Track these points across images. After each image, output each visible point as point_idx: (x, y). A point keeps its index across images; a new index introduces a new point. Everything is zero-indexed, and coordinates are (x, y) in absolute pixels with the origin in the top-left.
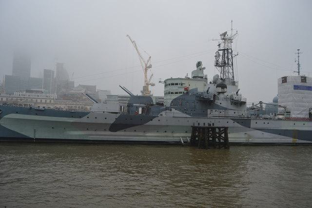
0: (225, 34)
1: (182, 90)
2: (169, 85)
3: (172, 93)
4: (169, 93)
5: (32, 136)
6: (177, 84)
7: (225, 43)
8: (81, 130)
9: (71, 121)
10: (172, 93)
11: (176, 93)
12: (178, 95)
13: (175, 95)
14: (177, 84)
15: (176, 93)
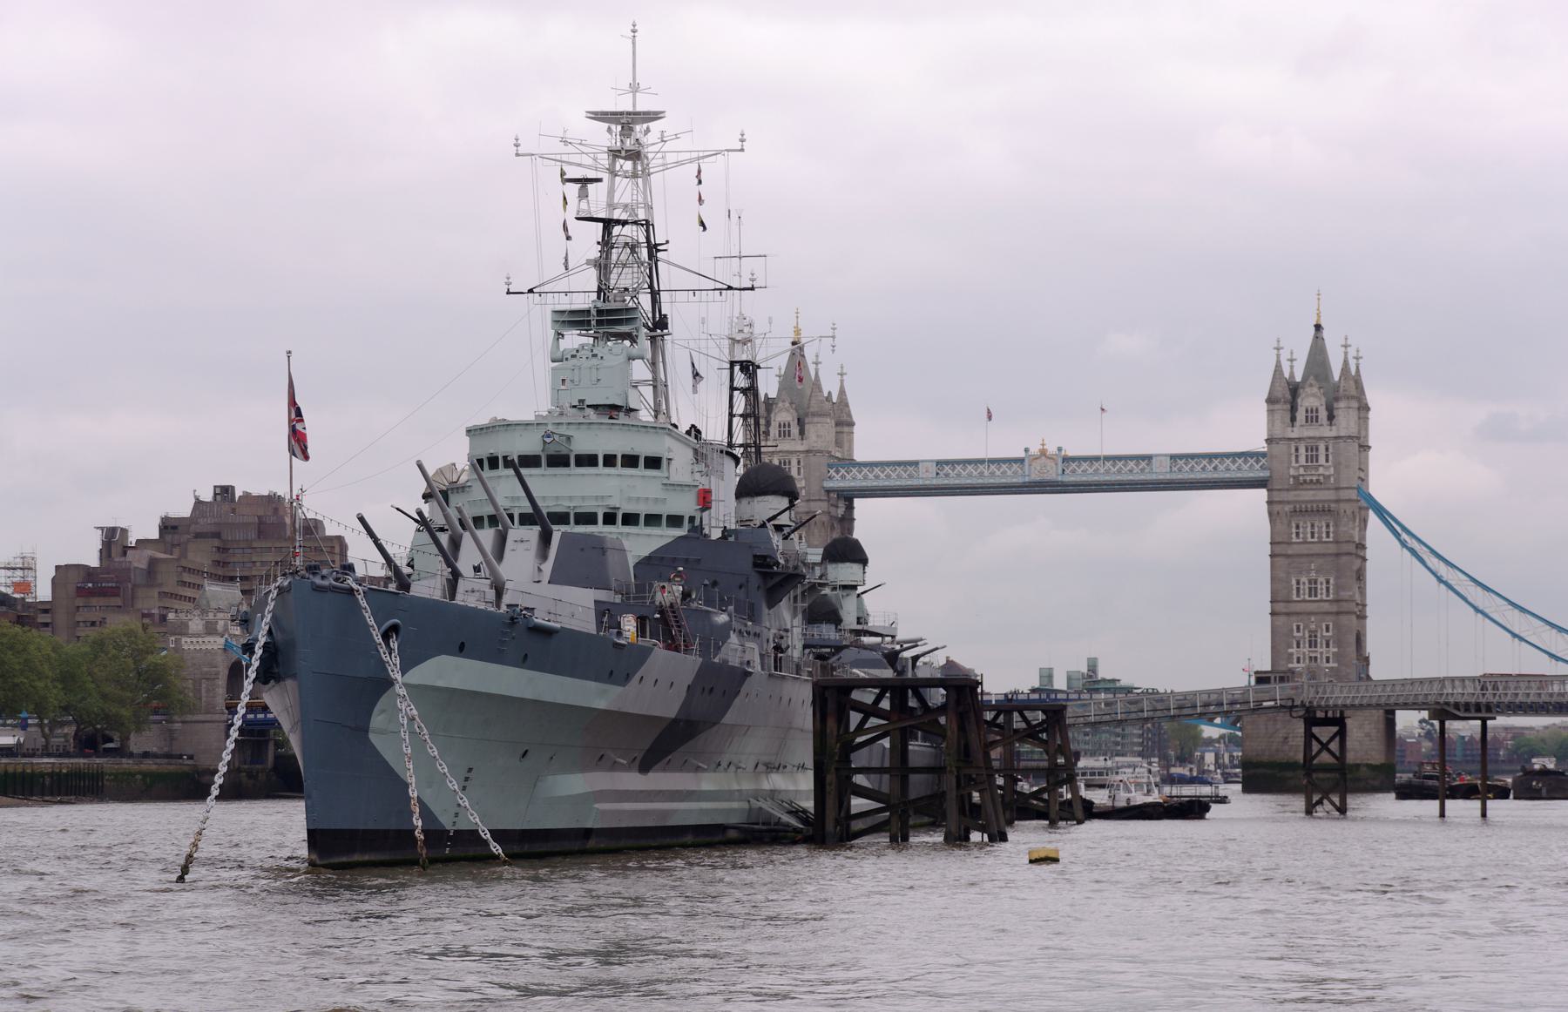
0: (627, 121)
1: (685, 505)
2: (610, 460)
3: (630, 519)
4: (610, 519)
5: (447, 822)
6: (654, 463)
7: (613, 173)
8: (585, 768)
9: (601, 704)
10: (630, 519)
11: (653, 520)
12: (664, 535)
13: (641, 529)
14: (654, 463)
15: (653, 520)
